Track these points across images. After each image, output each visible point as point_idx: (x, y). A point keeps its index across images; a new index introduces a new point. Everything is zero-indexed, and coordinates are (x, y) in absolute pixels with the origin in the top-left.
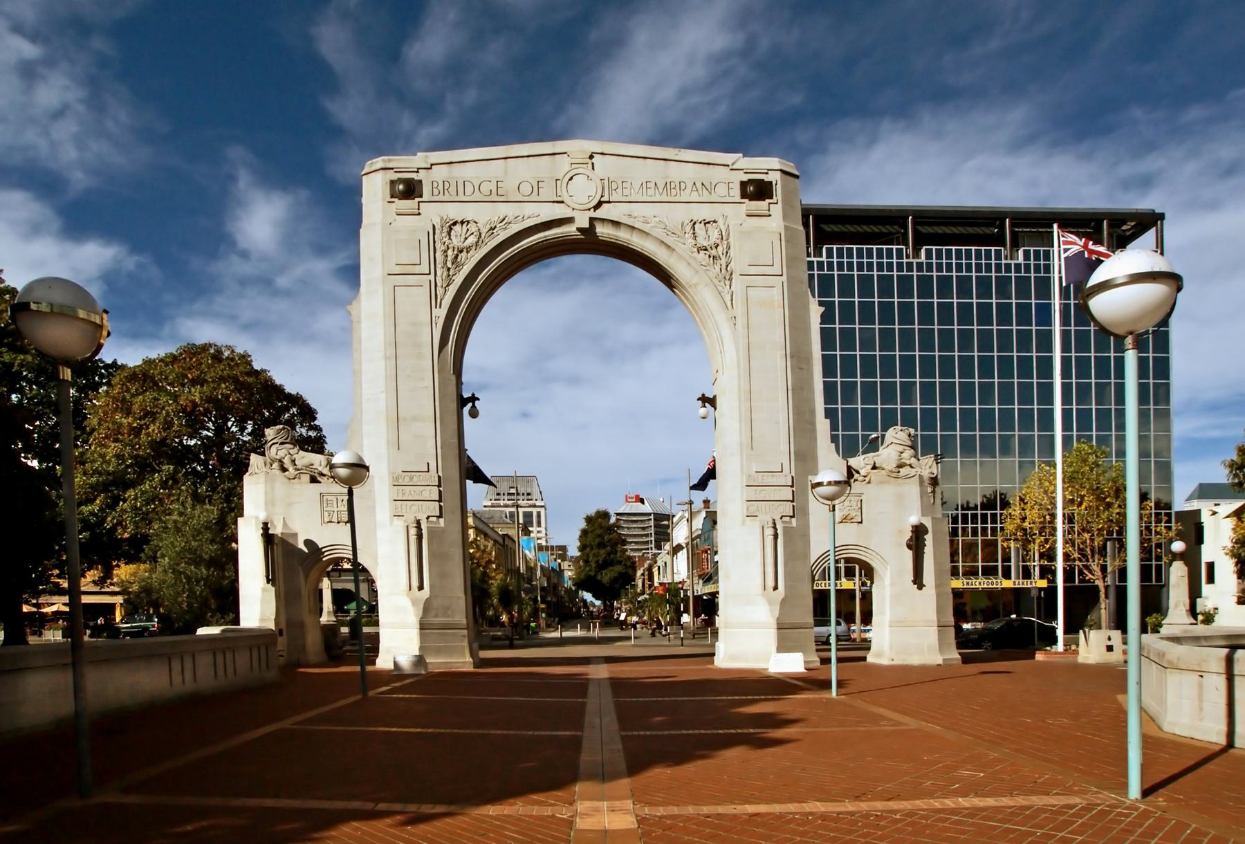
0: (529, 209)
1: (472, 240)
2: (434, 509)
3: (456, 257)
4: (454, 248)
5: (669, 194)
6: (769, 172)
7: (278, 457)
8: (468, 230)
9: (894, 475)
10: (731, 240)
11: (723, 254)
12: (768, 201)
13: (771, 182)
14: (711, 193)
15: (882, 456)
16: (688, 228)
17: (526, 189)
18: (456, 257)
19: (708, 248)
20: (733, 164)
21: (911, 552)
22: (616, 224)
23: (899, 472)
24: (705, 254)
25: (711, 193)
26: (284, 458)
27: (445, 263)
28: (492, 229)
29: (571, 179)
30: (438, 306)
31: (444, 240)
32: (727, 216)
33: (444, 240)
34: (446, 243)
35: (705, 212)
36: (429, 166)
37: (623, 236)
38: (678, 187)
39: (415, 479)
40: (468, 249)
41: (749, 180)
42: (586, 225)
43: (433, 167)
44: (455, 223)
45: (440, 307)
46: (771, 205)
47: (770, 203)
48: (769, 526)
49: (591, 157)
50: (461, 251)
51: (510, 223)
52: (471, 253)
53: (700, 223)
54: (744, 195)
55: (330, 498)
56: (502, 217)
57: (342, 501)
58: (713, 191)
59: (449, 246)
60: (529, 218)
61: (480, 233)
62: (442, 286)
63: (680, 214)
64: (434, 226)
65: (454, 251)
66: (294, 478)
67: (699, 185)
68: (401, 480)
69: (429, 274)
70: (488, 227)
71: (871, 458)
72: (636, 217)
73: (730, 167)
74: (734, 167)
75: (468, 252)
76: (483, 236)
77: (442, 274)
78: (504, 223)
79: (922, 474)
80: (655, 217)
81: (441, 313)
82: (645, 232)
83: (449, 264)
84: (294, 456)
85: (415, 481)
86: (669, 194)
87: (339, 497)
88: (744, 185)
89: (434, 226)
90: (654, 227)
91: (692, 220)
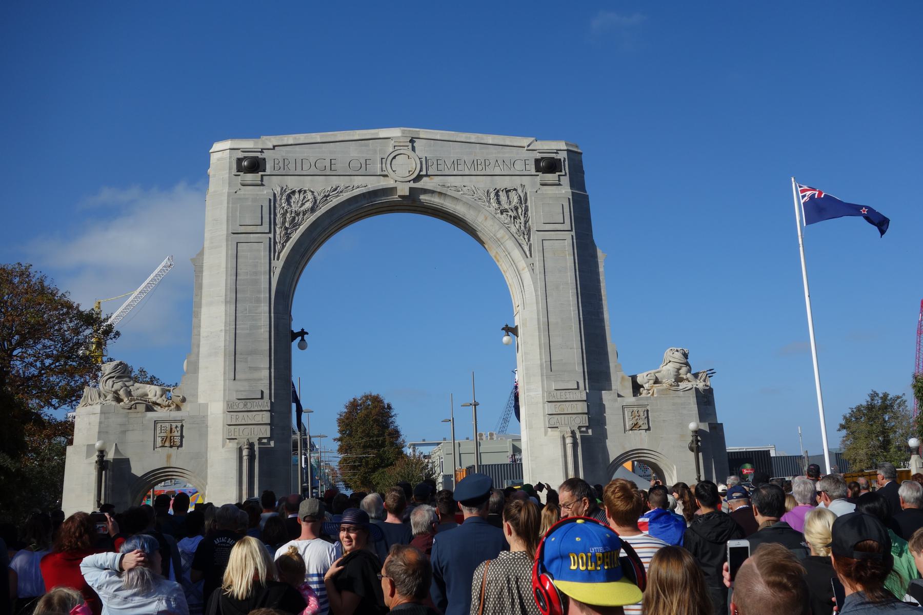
0: (358, 181)
1: (308, 205)
2: (266, 432)
3: (294, 218)
4: (292, 211)
5: (476, 169)
6: (558, 151)
7: (113, 389)
8: (304, 197)
9: (674, 388)
10: (529, 203)
11: (522, 214)
12: (558, 174)
13: (560, 160)
15: (662, 372)
16: (492, 195)
18: (294, 218)
19: (510, 211)
20: (528, 146)
21: (693, 453)
22: (432, 192)
23: (678, 386)
24: (507, 215)
26: (119, 390)
27: (284, 223)
28: (326, 196)
29: (394, 157)
30: (276, 259)
31: (283, 205)
32: (524, 186)
33: (283, 205)
34: (285, 208)
35: (505, 183)
36: (272, 148)
37: (436, 200)
38: (483, 164)
39: (249, 405)
40: (304, 213)
41: (542, 158)
42: (407, 193)
43: (276, 148)
44: (294, 192)
45: (278, 259)
46: (561, 177)
47: (559, 176)
48: (568, 435)
51: (341, 192)
52: (306, 216)
53: (503, 191)
54: (538, 169)
55: (163, 425)
56: (334, 187)
57: (176, 427)
58: (512, 166)
59: (288, 210)
60: (358, 187)
61: (315, 198)
62: (280, 242)
63: (483, 184)
64: (275, 195)
65: (291, 214)
66: (130, 409)
67: (500, 162)
68: (235, 407)
69: (270, 232)
70: (322, 195)
71: (653, 375)
72: (449, 187)
73: (526, 149)
74: (529, 148)
75: (304, 215)
76: (318, 201)
77: (281, 233)
78: (336, 192)
79: (697, 387)
80: (464, 186)
81: (279, 265)
82: (457, 198)
83: (287, 225)
84: (130, 388)
85: (249, 407)
86: (476, 169)
87: (174, 425)
88: (537, 161)
89: (275, 195)
90: (464, 194)
91: (496, 189)
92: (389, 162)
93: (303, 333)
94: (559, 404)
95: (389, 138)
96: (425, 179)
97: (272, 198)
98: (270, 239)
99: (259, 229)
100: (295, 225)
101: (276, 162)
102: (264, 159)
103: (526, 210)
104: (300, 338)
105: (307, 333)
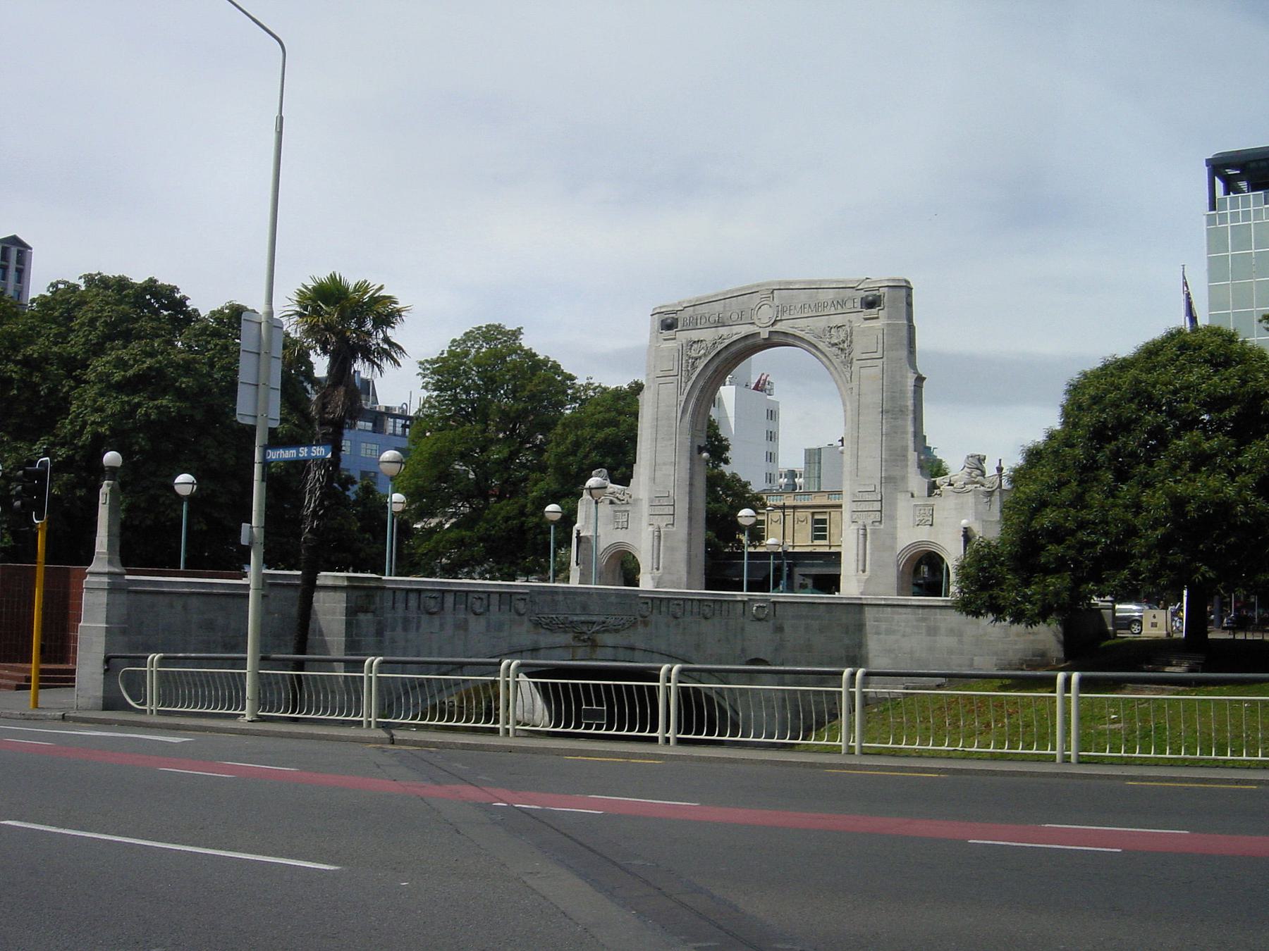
0: (736, 329)
1: (702, 352)
12: (878, 308)
17: (735, 317)
18: (693, 363)
29: (760, 308)
35: (837, 320)
39: (659, 501)
40: (700, 358)
44: (694, 342)
49: (772, 293)
50: (697, 359)
74: (858, 288)
92: (756, 312)
94: (859, 503)
95: (758, 292)
96: (779, 323)
97: (681, 349)
98: (678, 380)
99: (671, 373)
100: (694, 367)
102: (677, 319)
103: (851, 342)
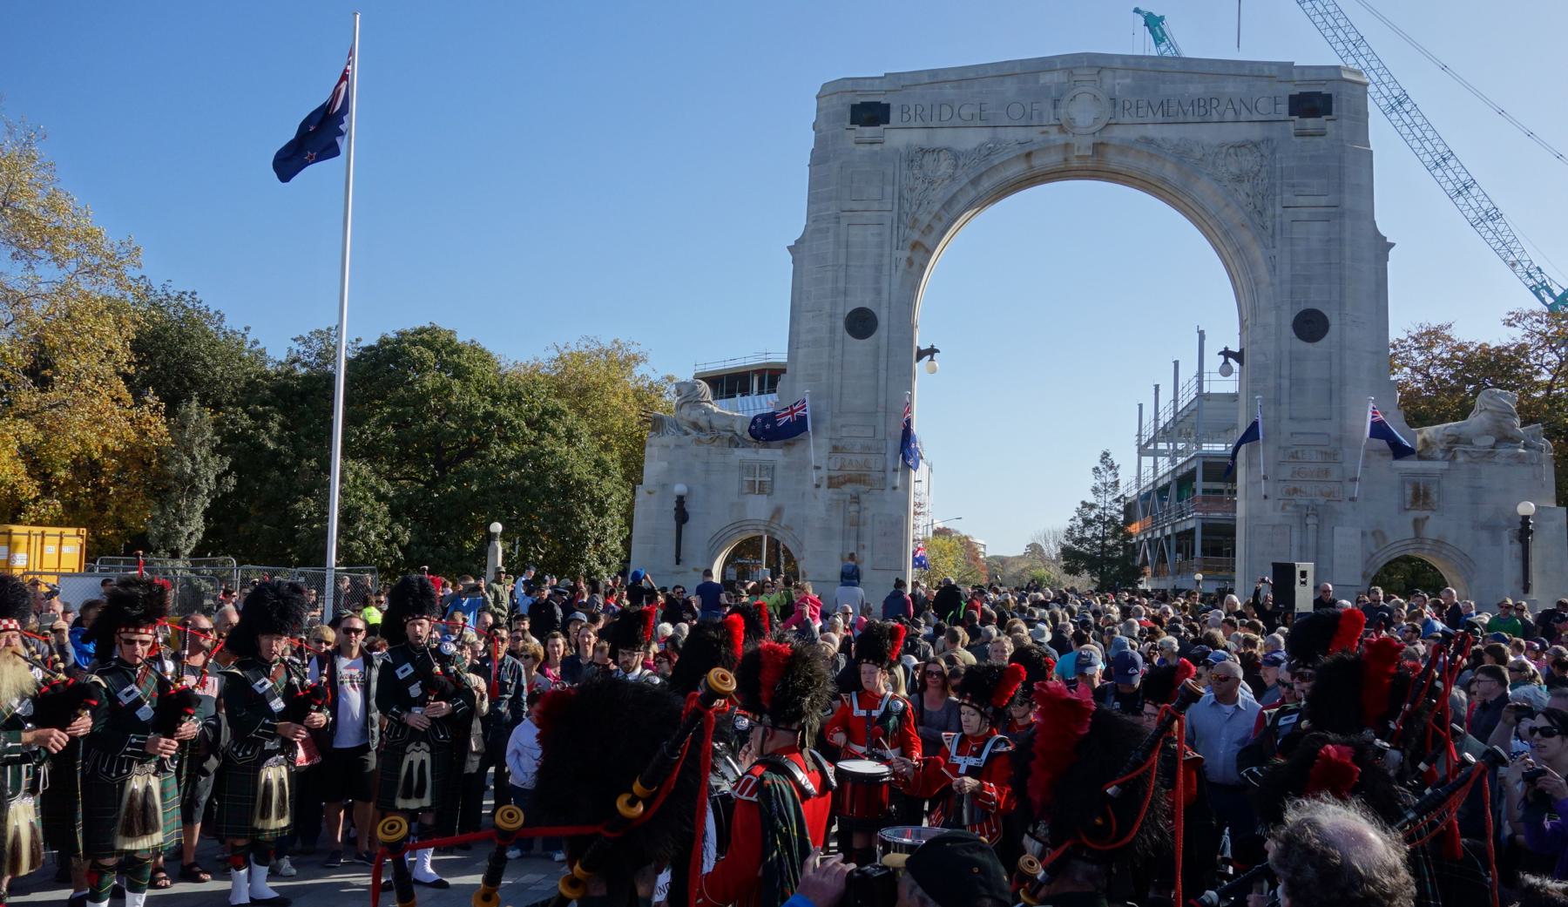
0: (1021, 134)
5: (1196, 113)
14: (1251, 112)
25: (1251, 112)
86: (1196, 113)
93: (932, 351)
96: (1115, 128)
101: (906, 110)
104: (928, 357)
105: (938, 351)
